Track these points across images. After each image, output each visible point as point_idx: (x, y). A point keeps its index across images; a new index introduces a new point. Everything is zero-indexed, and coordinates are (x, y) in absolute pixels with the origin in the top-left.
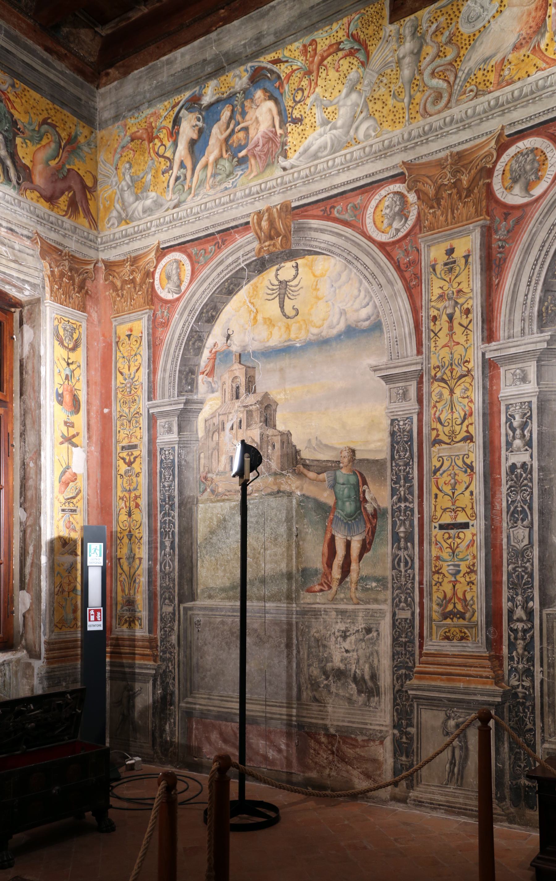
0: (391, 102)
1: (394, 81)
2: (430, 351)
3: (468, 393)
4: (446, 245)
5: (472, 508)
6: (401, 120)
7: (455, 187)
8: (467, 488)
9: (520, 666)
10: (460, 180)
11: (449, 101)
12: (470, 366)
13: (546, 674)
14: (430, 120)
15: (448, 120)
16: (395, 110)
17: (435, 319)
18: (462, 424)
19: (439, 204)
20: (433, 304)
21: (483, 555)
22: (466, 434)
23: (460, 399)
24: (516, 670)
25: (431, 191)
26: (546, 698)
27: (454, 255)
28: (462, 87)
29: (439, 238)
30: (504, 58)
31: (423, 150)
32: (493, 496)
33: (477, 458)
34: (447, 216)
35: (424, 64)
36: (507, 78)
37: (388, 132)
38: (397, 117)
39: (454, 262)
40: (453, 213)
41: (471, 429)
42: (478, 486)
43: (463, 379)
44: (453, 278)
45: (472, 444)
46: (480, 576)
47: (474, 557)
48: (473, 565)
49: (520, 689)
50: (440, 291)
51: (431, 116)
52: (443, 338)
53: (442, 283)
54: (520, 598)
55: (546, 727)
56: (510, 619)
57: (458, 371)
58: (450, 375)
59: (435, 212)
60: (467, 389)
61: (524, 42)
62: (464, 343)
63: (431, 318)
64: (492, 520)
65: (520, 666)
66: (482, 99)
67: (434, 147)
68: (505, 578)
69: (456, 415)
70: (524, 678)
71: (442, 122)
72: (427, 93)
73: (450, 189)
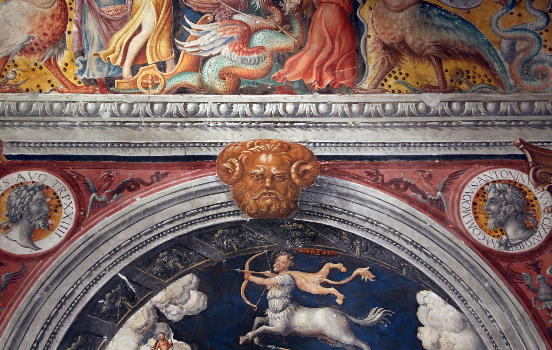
30: (7, 57)
36: (10, 82)
61: (35, 48)
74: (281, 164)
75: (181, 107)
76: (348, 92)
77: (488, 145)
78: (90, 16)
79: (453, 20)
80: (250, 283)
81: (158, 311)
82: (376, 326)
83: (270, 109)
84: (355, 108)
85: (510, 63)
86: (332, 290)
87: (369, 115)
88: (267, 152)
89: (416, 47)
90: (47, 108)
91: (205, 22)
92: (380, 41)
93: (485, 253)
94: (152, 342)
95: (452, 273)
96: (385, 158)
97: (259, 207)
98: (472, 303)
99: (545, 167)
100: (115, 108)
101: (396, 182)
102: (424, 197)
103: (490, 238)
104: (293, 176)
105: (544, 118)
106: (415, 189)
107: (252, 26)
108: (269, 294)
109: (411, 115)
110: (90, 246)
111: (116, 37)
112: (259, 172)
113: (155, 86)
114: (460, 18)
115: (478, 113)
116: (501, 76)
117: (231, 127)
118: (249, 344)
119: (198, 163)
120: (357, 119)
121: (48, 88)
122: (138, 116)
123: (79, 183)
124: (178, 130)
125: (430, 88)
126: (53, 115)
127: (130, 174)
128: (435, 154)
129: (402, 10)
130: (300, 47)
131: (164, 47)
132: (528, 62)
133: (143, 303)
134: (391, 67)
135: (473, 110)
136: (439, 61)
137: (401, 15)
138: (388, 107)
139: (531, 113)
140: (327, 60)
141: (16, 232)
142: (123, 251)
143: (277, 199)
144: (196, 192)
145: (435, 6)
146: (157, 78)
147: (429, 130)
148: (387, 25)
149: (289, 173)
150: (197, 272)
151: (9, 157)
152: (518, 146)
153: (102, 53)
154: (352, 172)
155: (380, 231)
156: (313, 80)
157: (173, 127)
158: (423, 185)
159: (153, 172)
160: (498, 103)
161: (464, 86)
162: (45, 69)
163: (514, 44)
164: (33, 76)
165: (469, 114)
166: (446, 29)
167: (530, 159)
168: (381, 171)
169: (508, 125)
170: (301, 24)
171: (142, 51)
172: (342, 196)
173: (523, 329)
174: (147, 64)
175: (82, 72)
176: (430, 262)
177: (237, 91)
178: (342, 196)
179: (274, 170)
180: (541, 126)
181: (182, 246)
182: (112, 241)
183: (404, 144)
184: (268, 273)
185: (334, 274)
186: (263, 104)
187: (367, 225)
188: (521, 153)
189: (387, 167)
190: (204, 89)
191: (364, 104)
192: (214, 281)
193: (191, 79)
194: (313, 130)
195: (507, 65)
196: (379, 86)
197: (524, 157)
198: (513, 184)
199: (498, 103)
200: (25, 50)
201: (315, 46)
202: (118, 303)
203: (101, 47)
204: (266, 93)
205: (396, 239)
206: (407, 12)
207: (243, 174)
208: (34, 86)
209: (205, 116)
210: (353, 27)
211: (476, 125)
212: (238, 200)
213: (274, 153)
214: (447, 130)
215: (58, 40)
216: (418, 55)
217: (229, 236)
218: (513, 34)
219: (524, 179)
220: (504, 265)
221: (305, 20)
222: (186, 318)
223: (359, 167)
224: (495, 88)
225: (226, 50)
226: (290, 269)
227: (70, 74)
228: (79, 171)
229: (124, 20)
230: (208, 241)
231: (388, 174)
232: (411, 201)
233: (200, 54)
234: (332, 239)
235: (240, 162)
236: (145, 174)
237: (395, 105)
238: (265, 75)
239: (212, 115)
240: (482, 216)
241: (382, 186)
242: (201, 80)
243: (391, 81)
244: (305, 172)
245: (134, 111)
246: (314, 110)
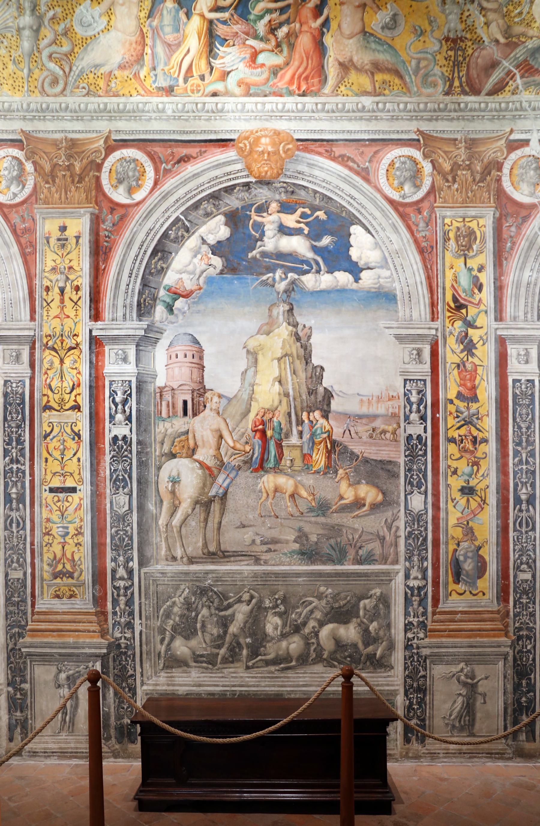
0: (11, 67)
1: (15, 47)
2: (42, 320)
3: (77, 365)
4: (60, 222)
5: (80, 474)
6: (21, 88)
7: (69, 170)
8: (74, 455)
9: (123, 620)
10: (74, 165)
11: (64, 89)
12: (79, 340)
13: (144, 626)
14: (47, 99)
15: (63, 105)
16: (15, 76)
17: (47, 289)
18: (70, 393)
19: (54, 181)
20: (46, 274)
21: (89, 518)
22: (74, 403)
23: (69, 370)
24: (119, 623)
25: (48, 168)
26: (144, 647)
27: (66, 233)
28: (75, 81)
29: (53, 213)
30: (111, 72)
31: (40, 126)
32: (98, 463)
33: (84, 426)
34: (61, 195)
35: (43, 43)
37: (7, 96)
38: (17, 83)
39: (66, 240)
40: (66, 194)
41: (79, 399)
42: (85, 453)
43: (72, 351)
44: (65, 254)
45: (79, 413)
46: (87, 538)
47: (82, 520)
48: (81, 528)
49: (123, 641)
50: (53, 264)
51: (48, 96)
52: (55, 310)
53: (55, 257)
54: (121, 558)
55: (144, 672)
56: (113, 578)
57: (69, 342)
58: (61, 346)
59: (50, 188)
60: (75, 361)
62: (74, 318)
63: (44, 287)
64: (97, 486)
65: (123, 620)
66: (92, 99)
67: (51, 126)
68: (108, 540)
69: (65, 384)
70: (126, 631)
71: (58, 106)
72: (45, 73)
73: (64, 171)
74: (274, 144)
75: (214, 106)
76: (316, 95)
77: (398, 132)
78: (159, 44)
79: (382, 45)
80: (254, 221)
81: (203, 239)
82: (326, 248)
83: (268, 107)
84: (320, 106)
85: (416, 76)
86: (302, 225)
87: (328, 112)
88: (266, 136)
89: (359, 65)
90: (135, 107)
91: (228, 46)
92: (337, 60)
93: (391, 202)
94: (199, 256)
95: (371, 214)
96: (337, 140)
97: (260, 173)
98: (381, 233)
99: (430, 146)
100: (174, 107)
101: (342, 156)
102: (358, 166)
103: (395, 192)
104: (281, 152)
105: (432, 114)
106: (354, 161)
107: (258, 49)
108: (266, 228)
109: (354, 111)
110: (163, 197)
111: (174, 57)
112: (260, 149)
113: (198, 91)
114: (387, 44)
115: (394, 111)
116: (409, 85)
117: (245, 120)
118: (254, 258)
119: (223, 143)
120: (322, 115)
121: (134, 93)
122: (188, 112)
123: (156, 157)
124: (212, 122)
125: (366, 93)
126: (139, 111)
127: (184, 151)
128: (366, 138)
129: (351, 38)
130: (287, 64)
131: (203, 63)
132: (426, 75)
133: (193, 233)
134: (343, 78)
135: (391, 108)
136: (373, 74)
137: (351, 41)
138: (340, 106)
139: (425, 111)
140: (303, 73)
141: (122, 189)
142: (182, 201)
143: (271, 168)
144: (224, 163)
145: (372, 35)
146: (199, 86)
147: (364, 122)
148: (342, 48)
149: (279, 150)
150: (225, 215)
151: (115, 141)
152: (415, 133)
153: (166, 69)
154: (316, 149)
155: (331, 188)
156: (294, 87)
157: (209, 119)
158: (358, 159)
159: (197, 150)
160: (406, 103)
161: (387, 92)
162: (133, 80)
163: (419, 63)
164: (126, 85)
165: (389, 111)
166: (378, 51)
167: (422, 142)
168: (334, 149)
169: (411, 119)
170: (288, 47)
171: (190, 67)
172: (310, 165)
173: (408, 248)
174: (192, 76)
175: (155, 82)
176: (359, 207)
177: (248, 94)
178: (310, 165)
179: (270, 149)
180: (430, 120)
181: (215, 197)
182: (175, 195)
183: (348, 131)
184: (265, 214)
185: (303, 216)
186: (264, 104)
187: (324, 184)
188: (417, 137)
189: (337, 146)
190: (227, 93)
191: (325, 104)
192: (234, 219)
193: (219, 87)
194: (294, 122)
195: (413, 77)
196: (335, 92)
197: (418, 140)
198: (410, 158)
199: (406, 103)
200: (121, 67)
201: (296, 63)
202: (180, 234)
203: (166, 64)
204: (266, 96)
205: (340, 193)
206: (355, 39)
207: (251, 152)
208: (127, 92)
209: (228, 112)
210: (320, 48)
211: (393, 119)
212: (248, 168)
213: (270, 137)
214: (374, 122)
215: (140, 59)
216: (359, 70)
217: (242, 191)
218: (419, 56)
219: (417, 155)
220: (401, 209)
221: (290, 44)
222: (219, 242)
223: (320, 146)
224: (405, 94)
225: (241, 66)
226: (278, 212)
227: (147, 84)
228: (155, 149)
229: (179, 45)
230: (230, 194)
231: (338, 151)
232: (351, 169)
233: (225, 69)
234: (303, 193)
235: (250, 143)
236: (192, 151)
237: (344, 104)
238: (265, 84)
239: (233, 112)
240: (391, 179)
241: (334, 159)
242: (226, 87)
243: (343, 88)
244: (288, 149)
245: (186, 109)
246: (294, 108)
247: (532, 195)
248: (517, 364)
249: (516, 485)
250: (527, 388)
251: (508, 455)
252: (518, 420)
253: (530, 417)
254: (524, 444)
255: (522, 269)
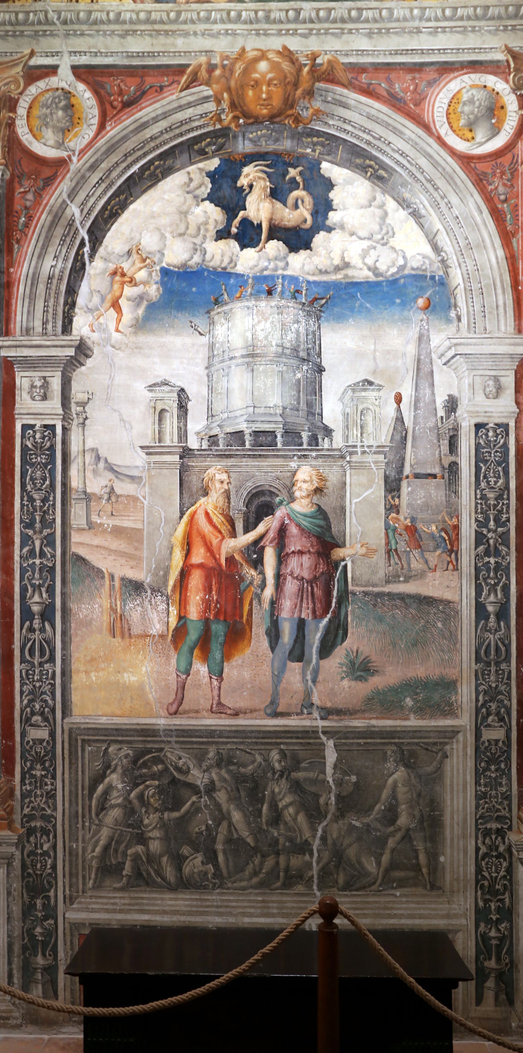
247: (59, 145)
248: (29, 401)
249: (24, 590)
250: (43, 438)
251: (13, 543)
252: (29, 488)
253: (48, 482)
254: (38, 525)
255: (41, 256)
